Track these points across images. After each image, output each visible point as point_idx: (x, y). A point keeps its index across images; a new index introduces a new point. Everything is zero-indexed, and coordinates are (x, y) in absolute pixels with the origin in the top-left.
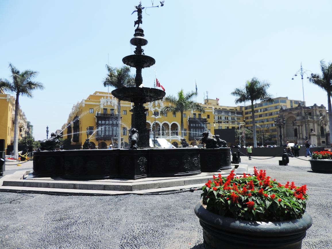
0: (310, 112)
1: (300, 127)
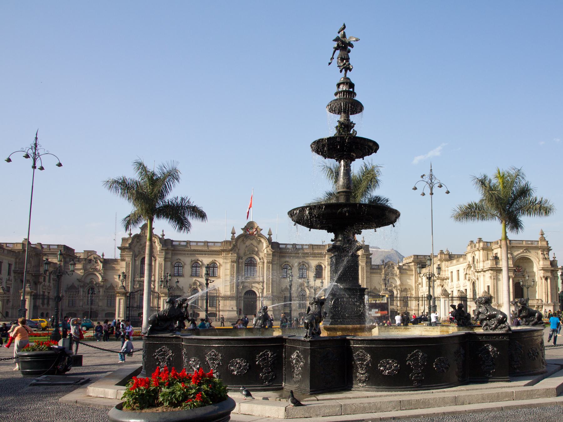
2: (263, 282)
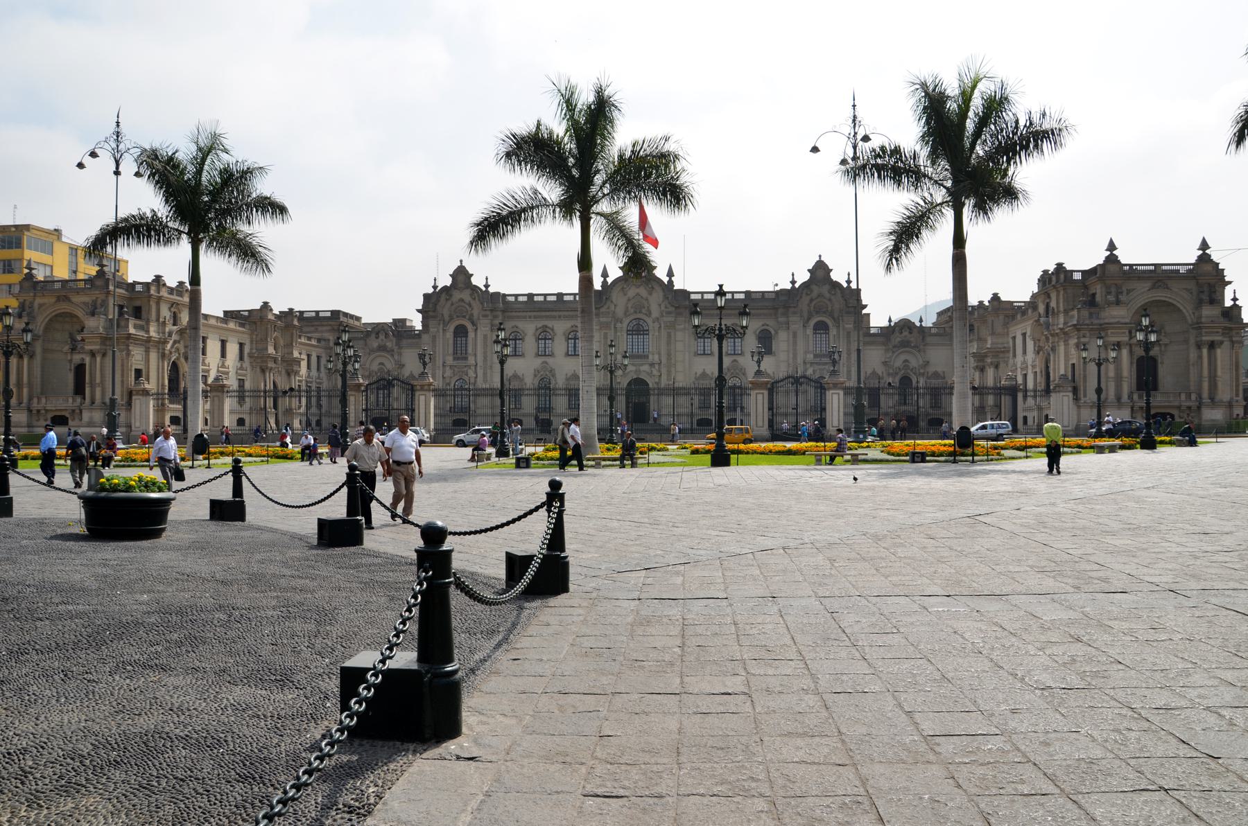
0: (137, 303)
1: (98, 359)
2: (660, 364)
